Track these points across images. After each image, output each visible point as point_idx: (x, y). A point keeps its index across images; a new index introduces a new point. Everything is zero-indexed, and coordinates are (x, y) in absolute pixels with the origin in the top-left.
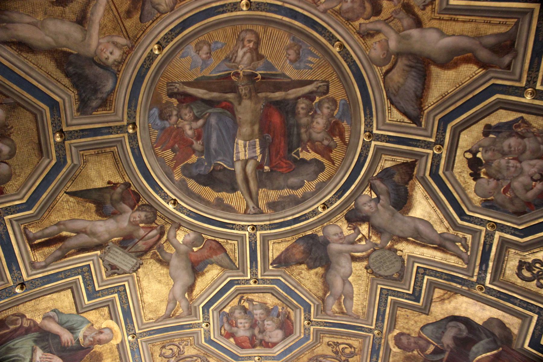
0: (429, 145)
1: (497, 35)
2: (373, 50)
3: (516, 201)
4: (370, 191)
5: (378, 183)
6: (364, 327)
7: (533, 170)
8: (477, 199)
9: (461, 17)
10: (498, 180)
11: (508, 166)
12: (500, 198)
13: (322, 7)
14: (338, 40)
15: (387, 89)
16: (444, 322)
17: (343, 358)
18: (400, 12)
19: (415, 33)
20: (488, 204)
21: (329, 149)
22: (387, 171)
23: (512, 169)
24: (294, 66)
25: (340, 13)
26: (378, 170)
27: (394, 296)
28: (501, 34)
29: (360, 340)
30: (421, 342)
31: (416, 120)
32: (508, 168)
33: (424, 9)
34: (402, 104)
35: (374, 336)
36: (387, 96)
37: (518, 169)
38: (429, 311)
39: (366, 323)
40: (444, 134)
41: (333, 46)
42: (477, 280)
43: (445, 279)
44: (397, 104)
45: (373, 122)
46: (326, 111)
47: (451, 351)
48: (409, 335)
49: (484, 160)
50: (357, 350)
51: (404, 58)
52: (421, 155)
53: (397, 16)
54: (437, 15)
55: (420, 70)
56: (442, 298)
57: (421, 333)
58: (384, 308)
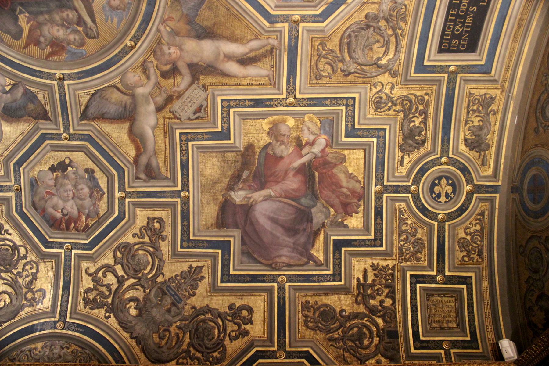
0: (66, 129)
1: (158, 167)
2: (133, 74)
3: (43, 202)
4: (11, 85)
5: (21, 90)
7: (69, 209)
8: (35, 173)
9: (168, 140)
10: (55, 186)
11: (67, 191)
12: (42, 190)
13: (162, 28)
14: (136, 44)
15: (104, 89)
18: (166, 93)
19: (152, 107)
20: (34, 182)
21: (37, 43)
22: (34, 97)
23: (66, 194)
24: (105, 5)
25: (159, 44)
26: (32, 89)
28: (159, 169)
31: (84, 116)
32: (66, 191)
33: (170, 112)
34: (94, 103)
36: (98, 90)
37: (67, 198)
40: (79, 139)
41: (130, 40)
44: (93, 99)
45: (73, 80)
46: (72, 37)
49: (67, 173)
51: (131, 100)
52: (56, 124)
53: (162, 91)
54: (167, 122)
55: (124, 114)
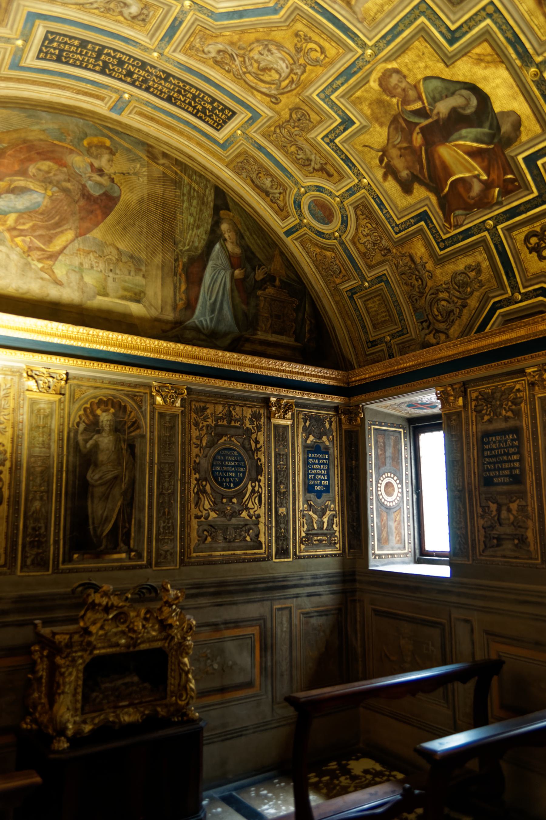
6: (358, 37)
16: (458, 86)
17: (302, 61)
27: (429, 19)
29: (341, 51)
30: (412, 94)
35: (363, 54)
38: (453, 63)
39: (367, 34)
42: (541, 63)
43: (507, 38)
47: (437, 121)
48: (405, 77)
50: (327, 60)
56: (482, 57)
57: (421, 83)
58: (404, 28)
